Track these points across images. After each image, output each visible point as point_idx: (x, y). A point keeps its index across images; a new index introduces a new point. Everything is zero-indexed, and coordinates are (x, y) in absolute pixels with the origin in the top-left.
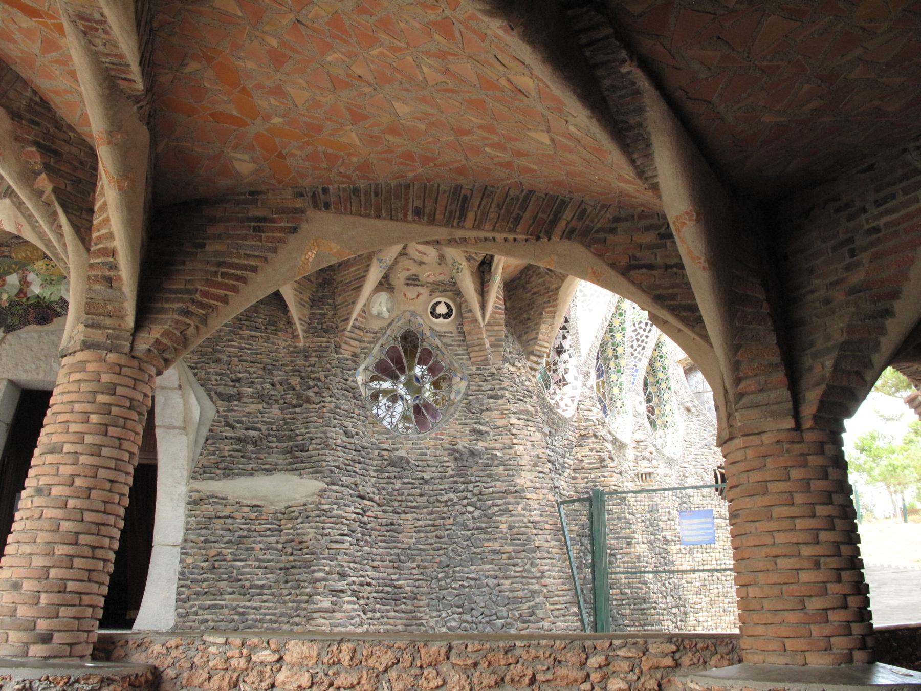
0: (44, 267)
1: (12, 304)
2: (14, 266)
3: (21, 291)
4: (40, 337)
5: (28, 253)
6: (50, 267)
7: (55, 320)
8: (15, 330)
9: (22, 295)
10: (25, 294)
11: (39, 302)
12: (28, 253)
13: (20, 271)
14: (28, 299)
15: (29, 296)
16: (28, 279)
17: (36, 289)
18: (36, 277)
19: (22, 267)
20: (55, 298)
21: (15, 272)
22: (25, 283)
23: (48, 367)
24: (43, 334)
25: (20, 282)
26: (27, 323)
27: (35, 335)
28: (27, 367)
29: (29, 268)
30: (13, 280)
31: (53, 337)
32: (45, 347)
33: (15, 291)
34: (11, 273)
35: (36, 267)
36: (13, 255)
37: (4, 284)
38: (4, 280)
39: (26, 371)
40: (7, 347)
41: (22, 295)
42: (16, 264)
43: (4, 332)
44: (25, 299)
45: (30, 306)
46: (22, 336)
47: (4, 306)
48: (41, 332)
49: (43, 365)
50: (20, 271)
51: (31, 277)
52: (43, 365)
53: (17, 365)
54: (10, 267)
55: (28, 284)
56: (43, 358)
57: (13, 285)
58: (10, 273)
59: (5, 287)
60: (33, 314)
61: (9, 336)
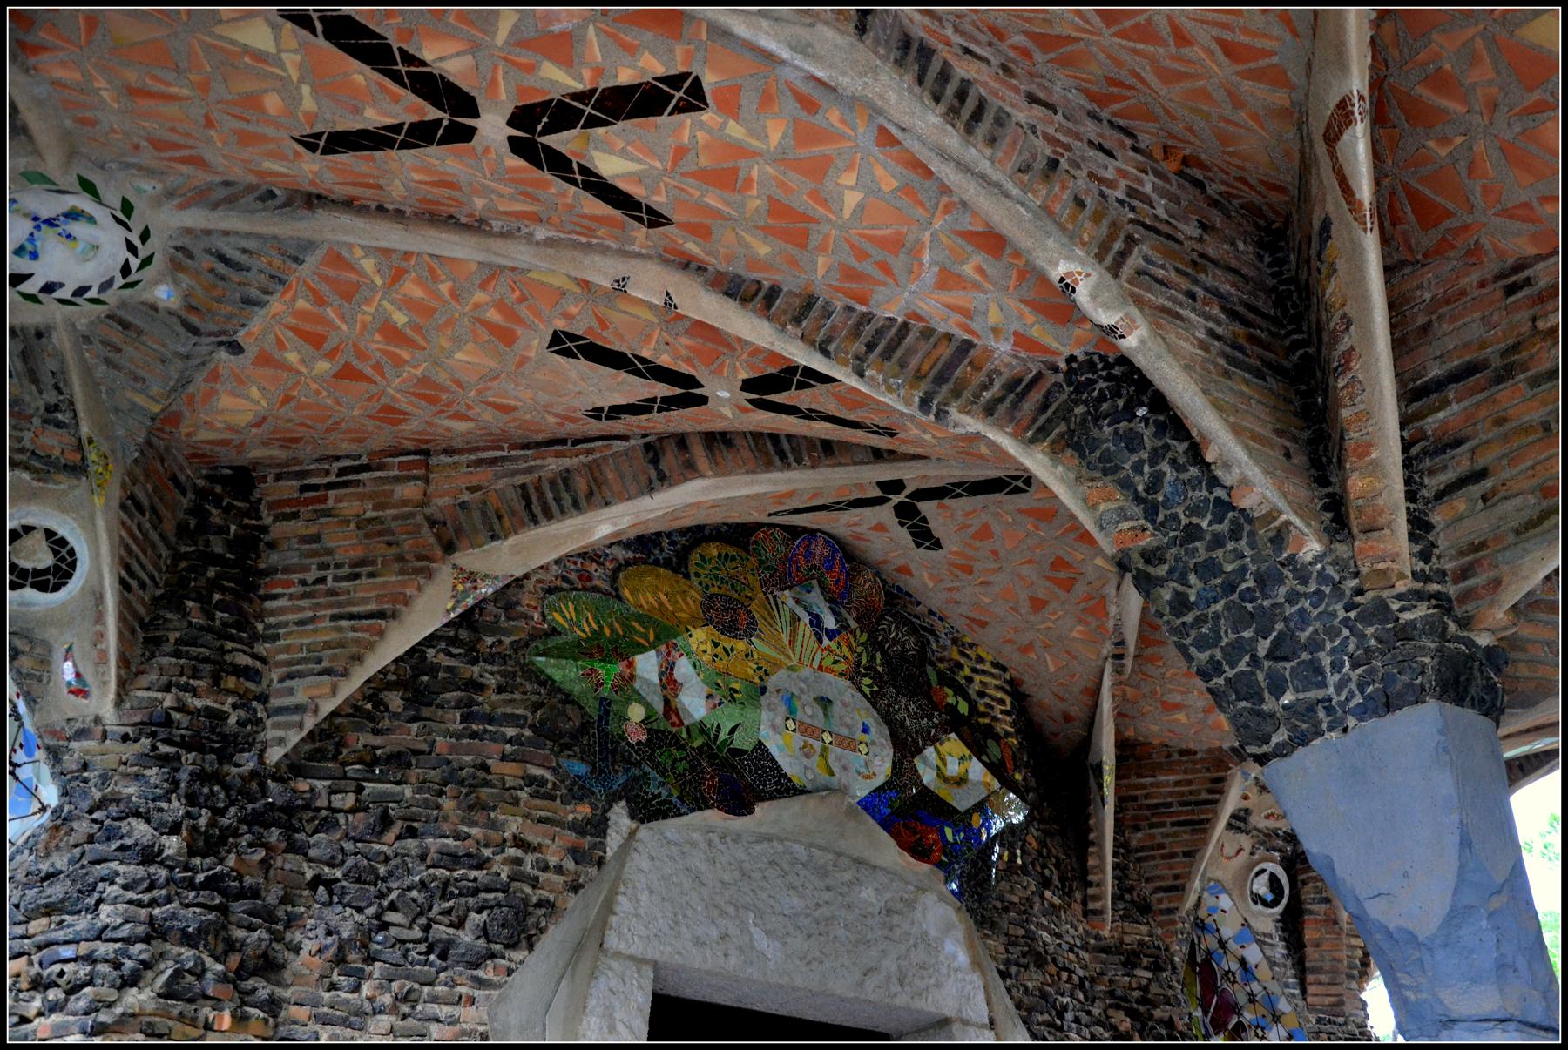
0: (709, 647)
6: (719, 650)
8: (666, 816)
12: (663, 598)
18: (691, 669)
20: (742, 741)
21: (653, 646)
22: (669, 683)
25: (661, 674)
26: (700, 804)
28: (699, 931)
29: (679, 641)
30: (647, 665)
36: (626, 593)
38: (631, 665)
39: (698, 942)
40: (645, 865)
43: (632, 817)
47: (633, 739)
49: (733, 931)
50: (663, 648)
51: (683, 668)
52: (733, 931)
56: (731, 910)
58: (642, 649)
60: (710, 785)
61: (644, 832)
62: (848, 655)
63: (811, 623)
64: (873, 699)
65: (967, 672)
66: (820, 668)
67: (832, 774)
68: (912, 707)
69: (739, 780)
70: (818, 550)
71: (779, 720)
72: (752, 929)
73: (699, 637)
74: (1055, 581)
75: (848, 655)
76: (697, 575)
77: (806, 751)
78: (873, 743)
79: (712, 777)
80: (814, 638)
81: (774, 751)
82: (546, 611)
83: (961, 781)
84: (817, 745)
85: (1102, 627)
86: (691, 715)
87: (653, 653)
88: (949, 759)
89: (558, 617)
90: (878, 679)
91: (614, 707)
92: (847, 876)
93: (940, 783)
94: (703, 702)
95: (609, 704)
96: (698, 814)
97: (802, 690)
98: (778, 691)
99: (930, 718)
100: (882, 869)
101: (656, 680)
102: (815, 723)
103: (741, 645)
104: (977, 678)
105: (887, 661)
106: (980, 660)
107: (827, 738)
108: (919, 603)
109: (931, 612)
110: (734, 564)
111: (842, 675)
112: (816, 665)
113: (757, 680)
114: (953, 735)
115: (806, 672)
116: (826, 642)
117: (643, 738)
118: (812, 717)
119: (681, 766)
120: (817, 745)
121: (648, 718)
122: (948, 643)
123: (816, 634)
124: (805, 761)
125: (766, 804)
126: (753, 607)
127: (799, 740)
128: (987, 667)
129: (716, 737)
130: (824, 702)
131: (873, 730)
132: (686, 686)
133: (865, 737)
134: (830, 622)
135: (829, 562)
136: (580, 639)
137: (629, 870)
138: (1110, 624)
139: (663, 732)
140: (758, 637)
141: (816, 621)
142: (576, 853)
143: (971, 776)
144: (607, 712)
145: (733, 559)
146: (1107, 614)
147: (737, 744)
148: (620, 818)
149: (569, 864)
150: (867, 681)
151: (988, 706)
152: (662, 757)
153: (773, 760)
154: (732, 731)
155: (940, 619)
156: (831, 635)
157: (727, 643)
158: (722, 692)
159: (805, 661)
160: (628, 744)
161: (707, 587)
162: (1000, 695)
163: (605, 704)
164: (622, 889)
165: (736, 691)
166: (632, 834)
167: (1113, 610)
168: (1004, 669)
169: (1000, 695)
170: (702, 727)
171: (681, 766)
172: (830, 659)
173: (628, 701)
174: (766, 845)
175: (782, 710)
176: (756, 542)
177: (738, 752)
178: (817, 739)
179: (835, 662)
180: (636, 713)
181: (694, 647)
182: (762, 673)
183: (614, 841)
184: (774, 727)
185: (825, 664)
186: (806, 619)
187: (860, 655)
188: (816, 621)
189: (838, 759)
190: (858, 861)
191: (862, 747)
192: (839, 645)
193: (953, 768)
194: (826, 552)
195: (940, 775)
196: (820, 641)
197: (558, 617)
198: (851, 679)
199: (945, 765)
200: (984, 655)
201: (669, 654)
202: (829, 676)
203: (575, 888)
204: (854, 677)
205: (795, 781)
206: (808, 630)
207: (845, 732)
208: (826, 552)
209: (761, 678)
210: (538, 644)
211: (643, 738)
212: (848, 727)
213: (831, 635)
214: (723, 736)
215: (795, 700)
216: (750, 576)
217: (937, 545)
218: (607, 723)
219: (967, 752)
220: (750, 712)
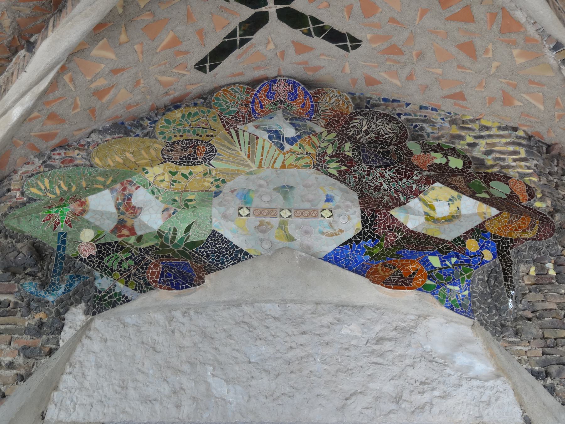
0: (167, 177)
1: (104, 249)
2: (100, 179)
3: (121, 225)
4: (171, 320)
5: (129, 155)
6: (178, 177)
7: (207, 278)
8: (114, 305)
9: (125, 232)
10: (132, 231)
11: (162, 245)
12: (129, 155)
13: (118, 186)
14: (140, 239)
15: (139, 233)
16: (134, 202)
17: (152, 218)
18: (150, 196)
19: (121, 178)
20: (199, 235)
21: (106, 187)
22: (127, 207)
23: (202, 388)
24: (178, 314)
26: (144, 287)
27: (159, 317)
28: (150, 391)
29: (135, 179)
30: (103, 203)
31: (202, 321)
32: (186, 342)
33: (109, 225)
34: (99, 190)
35: (150, 177)
36: (97, 160)
37: (84, 211)
38: (83, 204)
39: (146, 400)
40: (96, 346)
41: (125, 232)
42: (105, 175)
43: (86, 313)
44: (132, 240)
45: (147, 250)
46: (128, 320)
48: (171, 308)
49: (188, 384)
50: (118, 186)
51: (140, 197)
52: (188, 384)
53: (124, 387)
54: (92, 181)
55: (135, 211)
56: (186, 368)
57: (102, 213)
59: (87, 217)
60: (154, 270)
61: (99, 322)
62: (311, 151)
63: (270, 138)
64: (341, 177)
65: (470, 140)
66: (283, 166)
67: (291, 239)
68: (388, 174)
69: (183, 264)
70: (281, 89)
71: (232, 211)
72: (210, 380)
73: (157, 173)
74: (452, 18)
75: (311, 151)
76: (161, 133)
77: (262, 228)
78: (338, 207)
79: (156, 266)
80: (274, 147)
81: (228, 235)
82: (25, 189)
83: (451, 219)
84: (275, 221)
85: (528, 39)
86: (147, 227)
87: (107, 192)
88: (436, 204)
89: (34, 190)
90: (349, 162)
91: (69, 237)
92: (327, 319)
93: (427, 224)
94: (159, 215)
95: (65, 236)
96: (144, 297)
97: (260, 186)
98: (232, 192)
99: (409, 177)
100: (370, 307)
101: (114, 210)
102: (273, 206)
103: (200, 169)
104: (482, 142)
105: (358, 147)
106: (488, 128)
107: (285, 214)
108: (408, 105)
109: (421, 108)
110: (196, 118)
111: (306, 166)
112: (278, 164)
113: (213, 189)
114: (437, 184)
115: (267, 172)
116: (287, 147)
117: (94, 252)
118: (270, 201)
119: (125, 265)
120: (275, 221)
121: (96, 237)
122: (447, 125)
123: (276, 144)
124: (261, 236)
125: (212, 275)
126: (214, 142)
127: (254, 221)
128: (494, 131)
129: (174, 238)
130: (285, 190)
131: (337, 199)
132: (145, 209)
133: (330, 205)
134: (289, 132)
135: (293, 96)
136: (53, 199)
137: (79, 354)
138: (531, 31)
139: (110, 244)
140: (218, 159)
141: (276, 135)
142: (28, 352)
143: (464, 212)
144: (64, 242)
145: (196, 114)
146: (519, 24)
147: (191, 239)
148: (76, 316)
149: (20, 360)
150: (334, 165)
151: (496, 159)
152: (109, 262)
153: (228, 241)
154: (188, 229)
155: (432, 109)
156: (291, 141)
157: (184, 169)
158: (180, 203)
159: (265, 164)
160: (81, 260)
161: (170, 138)
162: (511, 148)
163: (62, 239)
164: (68, 369)
165: (191, 200)
166: (87, 326)
167: (520, 16)
168: (515, 129)
169: (511, 148)
170: (160, 234)
171: (125, 265)
172: (294, 157)
173: (80, 230)
174: (234, 310)
175: (239, 202)
176: (218, 99)
177: (194, 244)
178: (274, 216)
179: (298, 159)
180: (87, 235)
181: (151, 180)
182: (219, 183)
183: (67, 334)
184: (225, 217)
185: (287, 163)
186: (265, 136)
187: (326, 148)
188: (276, 135)
189: (298, 227)
190: (341, 306)
191: (326, 213)
192: (301, 146)
193: (442, 210)
194: (289, 88)
195: (429, 218)
196: (282, 148)
197: (34, 190)
198: (316, 167)
199: (432, 208)
200: (489, 124)
201: (124, 189)
202: (294, 170)
203: (22, 378)
204: (319, 165)
205: (251, 253)
206: (268, 144)
207: (307, 205)
208: (289, 88)
209: (218, 186)
210: (18, 212)
211: (94, 252)
212: (309, 201)
213: (291, 141)
214: (179, 235)
215: (251, 195)
216: (211, 122)
217: (356, 43)
218: (64, 249)
219: (455, 193)
220: (202, 211)
